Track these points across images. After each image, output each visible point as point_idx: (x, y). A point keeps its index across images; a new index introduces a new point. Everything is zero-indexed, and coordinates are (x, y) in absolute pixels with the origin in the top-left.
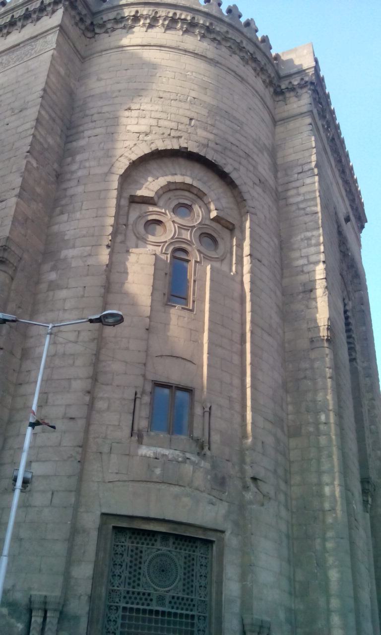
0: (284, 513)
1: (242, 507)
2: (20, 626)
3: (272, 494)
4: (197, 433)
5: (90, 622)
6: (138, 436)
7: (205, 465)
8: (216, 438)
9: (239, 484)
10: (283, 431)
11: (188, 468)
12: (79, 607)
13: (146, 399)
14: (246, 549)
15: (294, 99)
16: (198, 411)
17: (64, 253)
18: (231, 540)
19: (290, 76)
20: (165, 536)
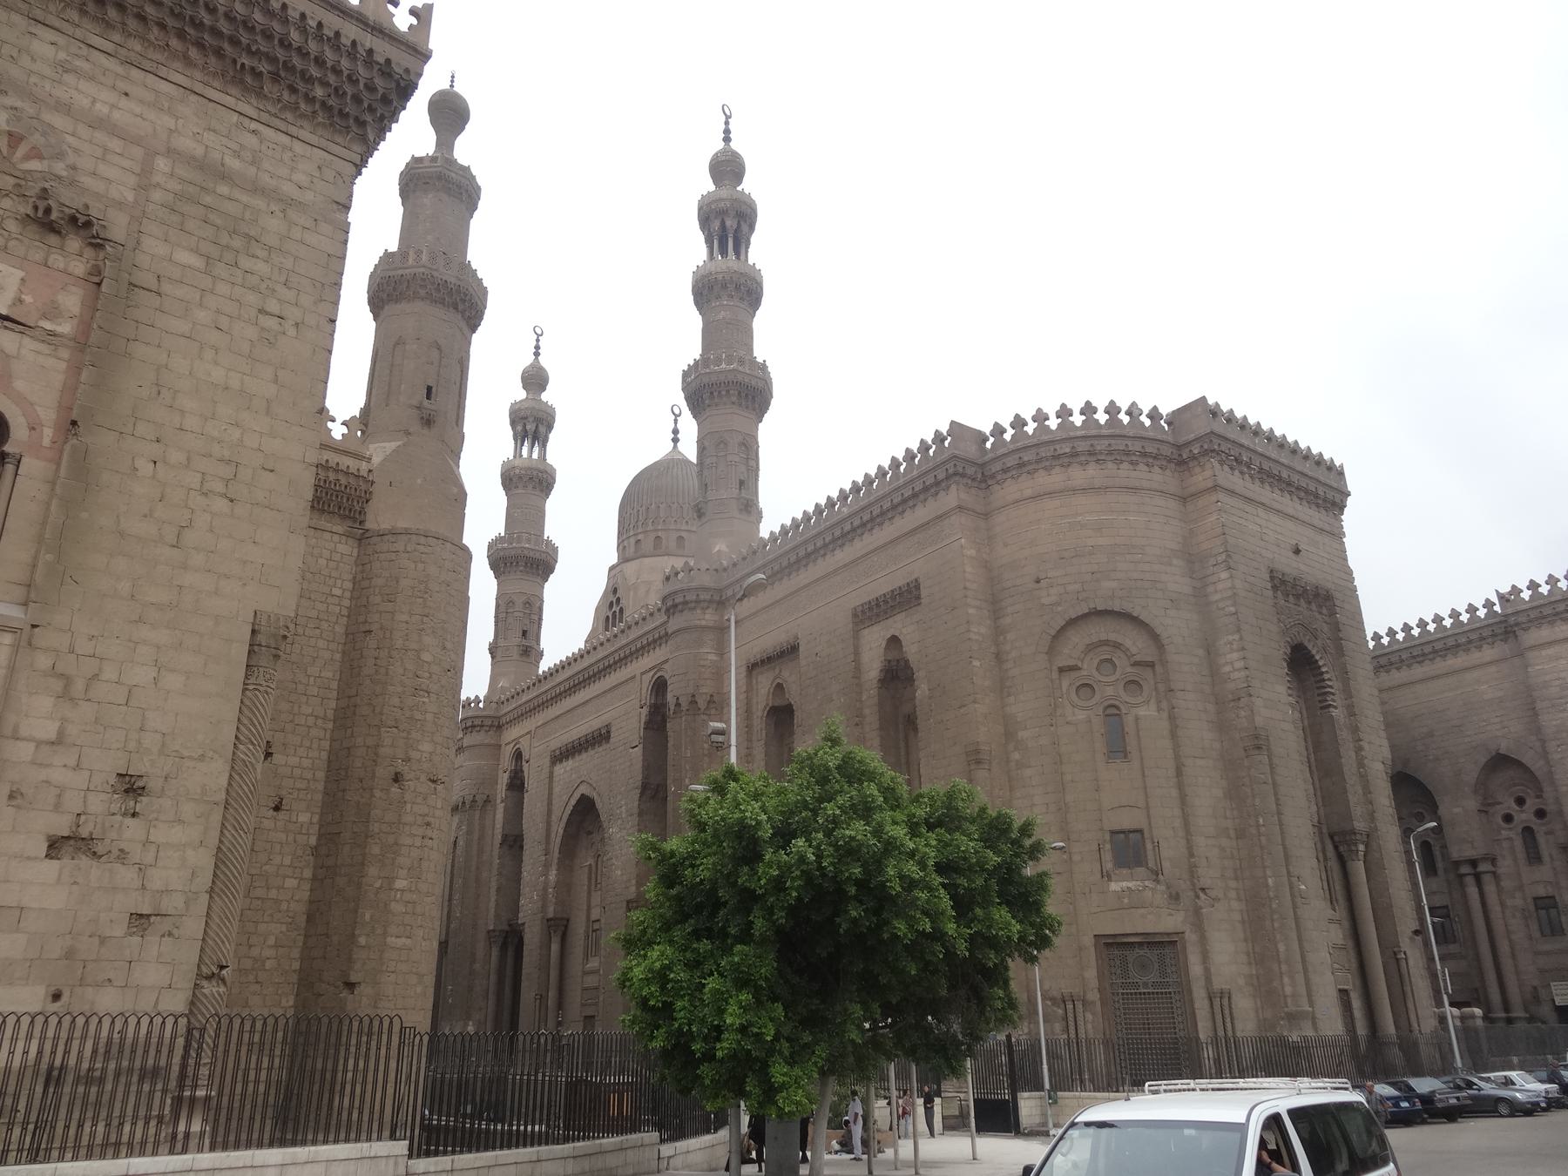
0: (1235, 905)
1: (1197, 911)
2: (1060, 1011)
3: (1221, 895)
4: (1151, 864)
5: (1102, 1004)
6: (1107, 876)
7: (1162, 888)
8: (1166, 864)
9: (1191, 894)
10: (1229, 837)
11: (1148, 893)
12: (1094, 996)
13: (1108, 846)
14: (1203, 940)
15: (1197, 470)
16: (1149, 846)
17: (1021, 734)
18: (1191, 937)
19: (1189, 443)
20: (1140, 944)
